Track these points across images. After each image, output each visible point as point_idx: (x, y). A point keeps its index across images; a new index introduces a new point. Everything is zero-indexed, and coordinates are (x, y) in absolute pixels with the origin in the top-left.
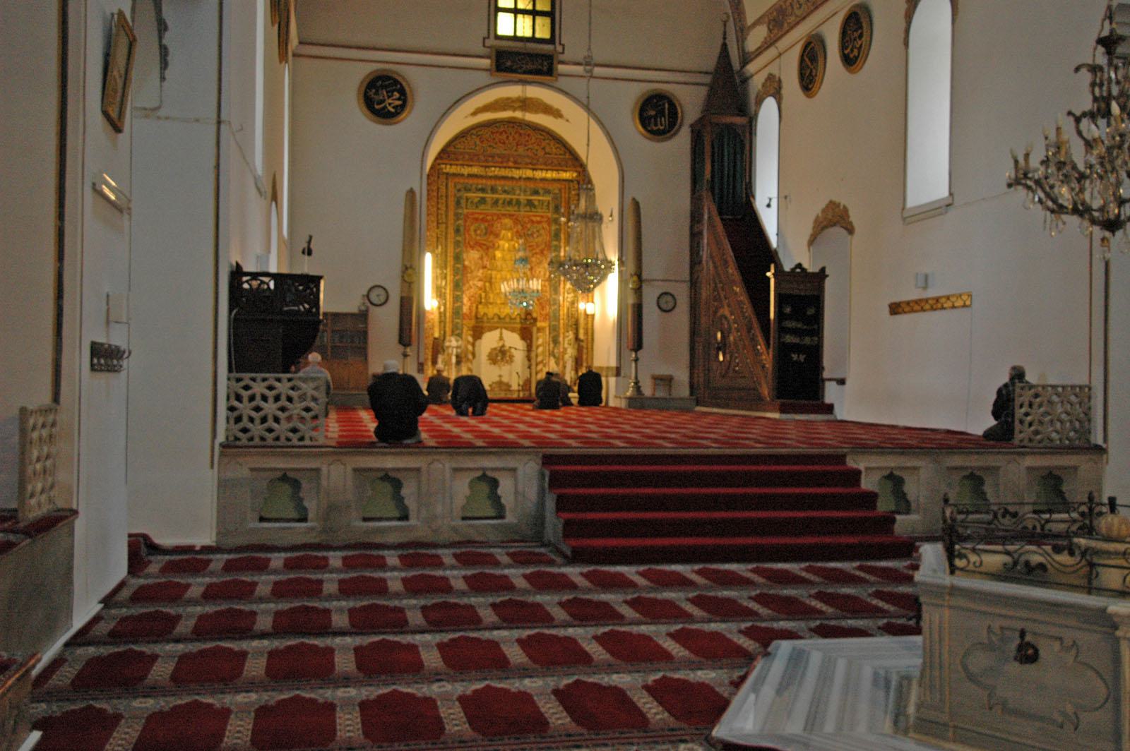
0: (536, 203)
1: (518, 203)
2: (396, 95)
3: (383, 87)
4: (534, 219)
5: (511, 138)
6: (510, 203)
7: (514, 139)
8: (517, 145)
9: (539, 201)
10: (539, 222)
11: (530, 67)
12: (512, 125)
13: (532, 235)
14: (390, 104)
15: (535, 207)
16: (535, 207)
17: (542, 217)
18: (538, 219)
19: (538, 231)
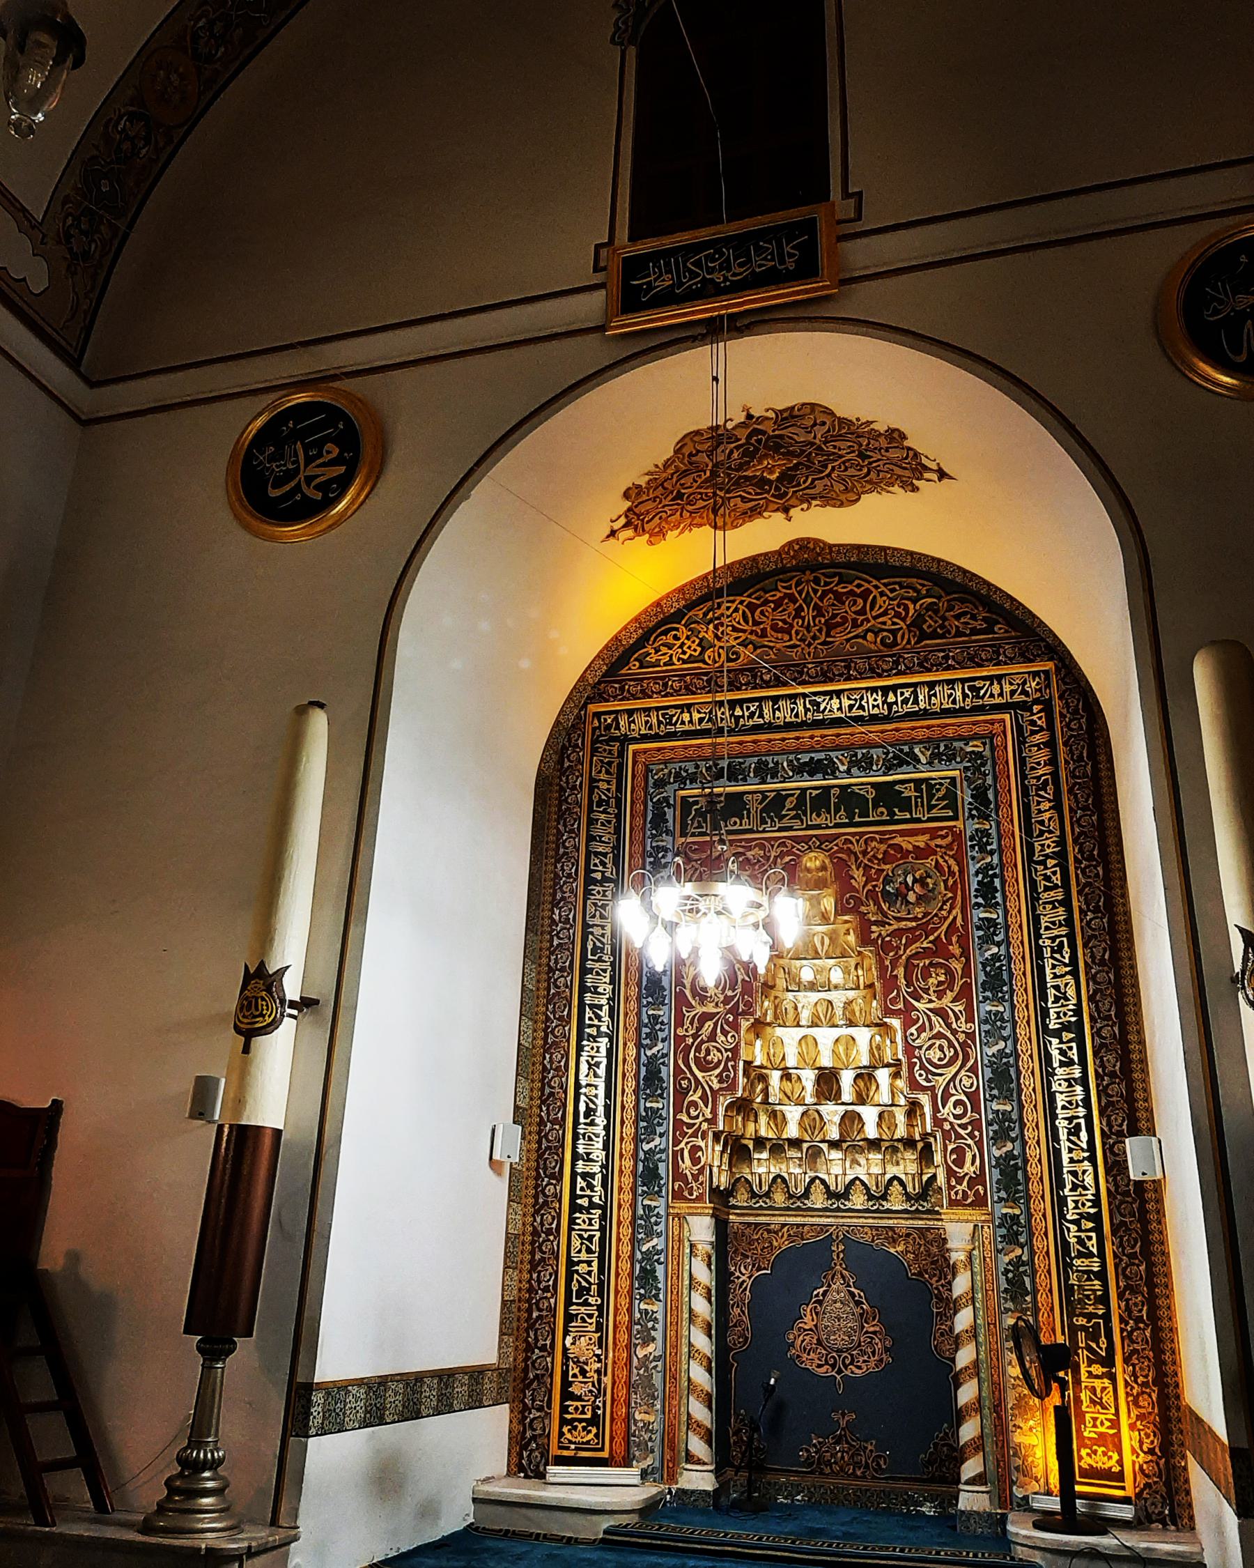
0: (909, 792)
1: (849, 798)
2: (333, 450)
3: (297, 435)
4: (906, 843)
5: (809, 613)
6: (821, 801)
7: (819, 611)
8: (830, 627)
9: (918, 783)
10: (921, 853)
11: (739, 272)
12: (809, 576)
13: (901, 895)
14: (309, 480)
15: (905, 805)
16: (905, 805)
17: (933, 833)
18: (921, 841)
19: (921, 881)
